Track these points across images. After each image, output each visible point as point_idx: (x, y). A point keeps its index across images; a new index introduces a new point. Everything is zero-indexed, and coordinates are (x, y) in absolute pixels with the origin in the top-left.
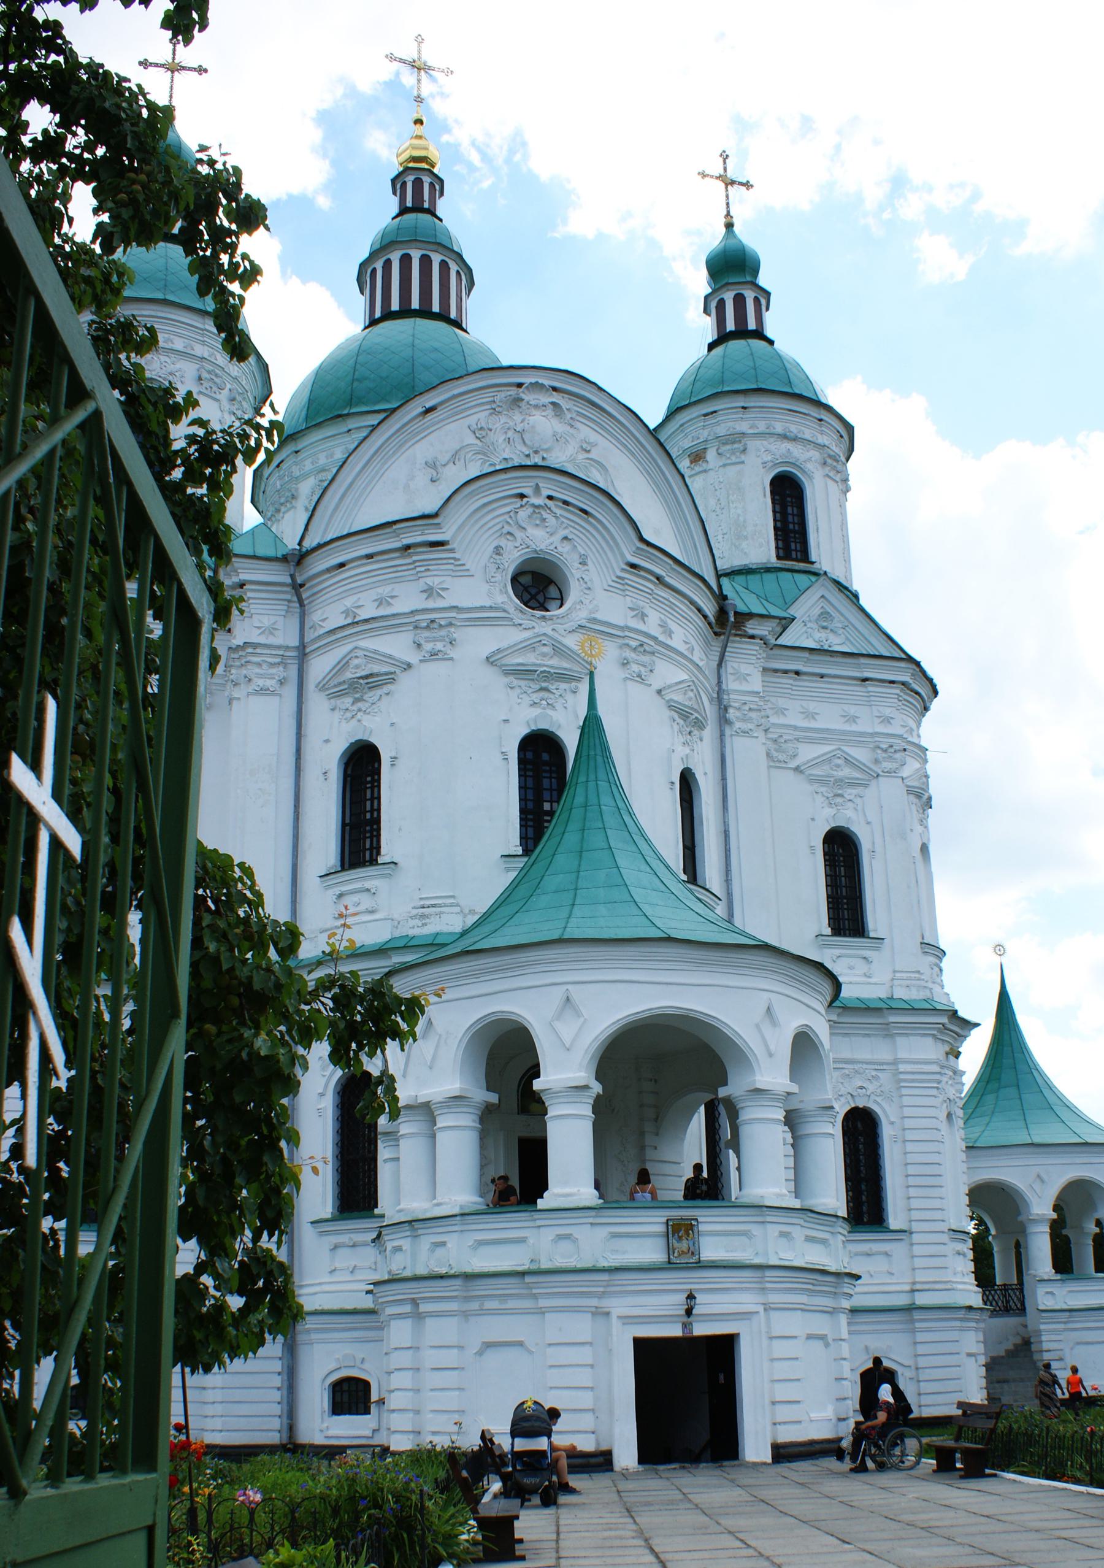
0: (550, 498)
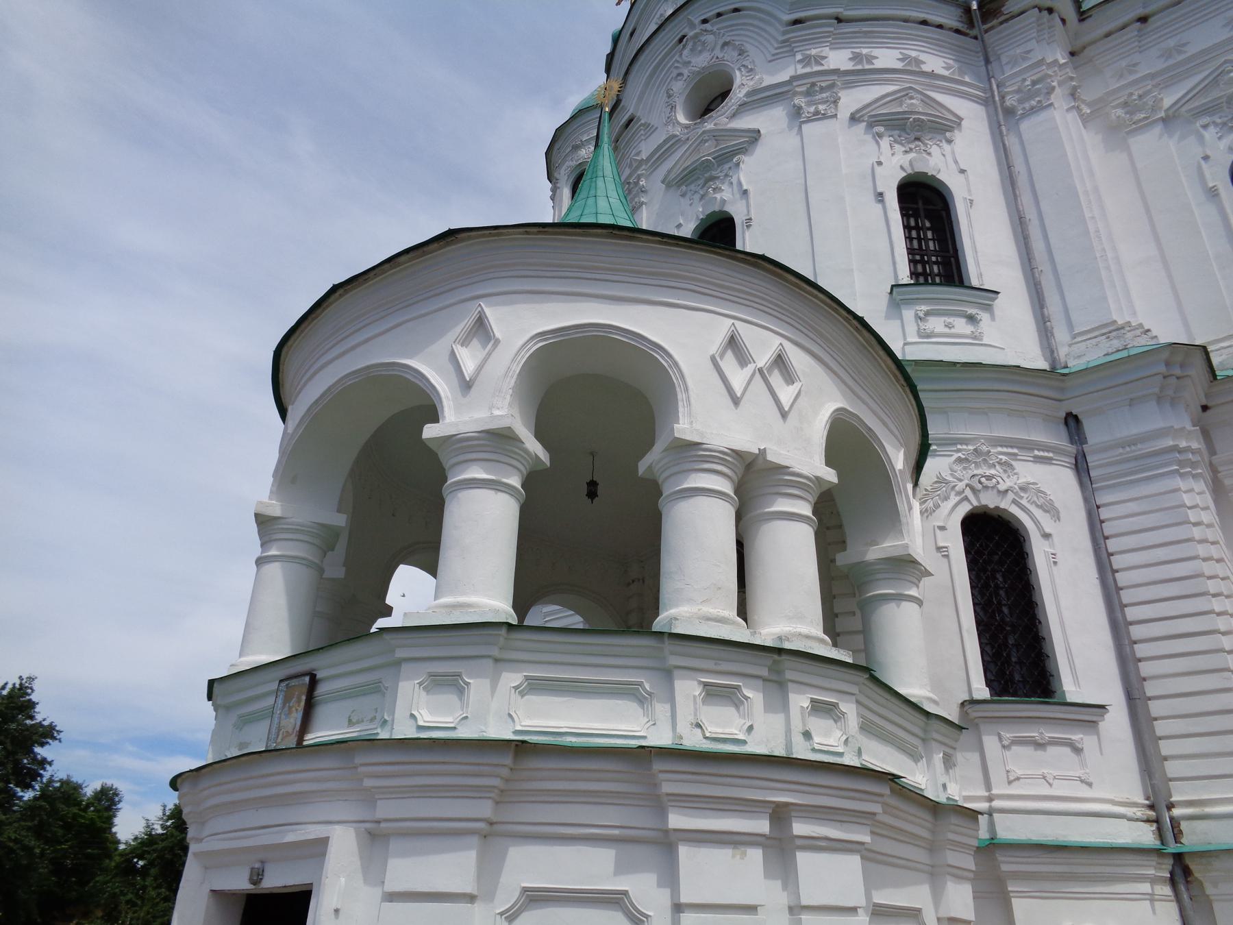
0: (705, 21)
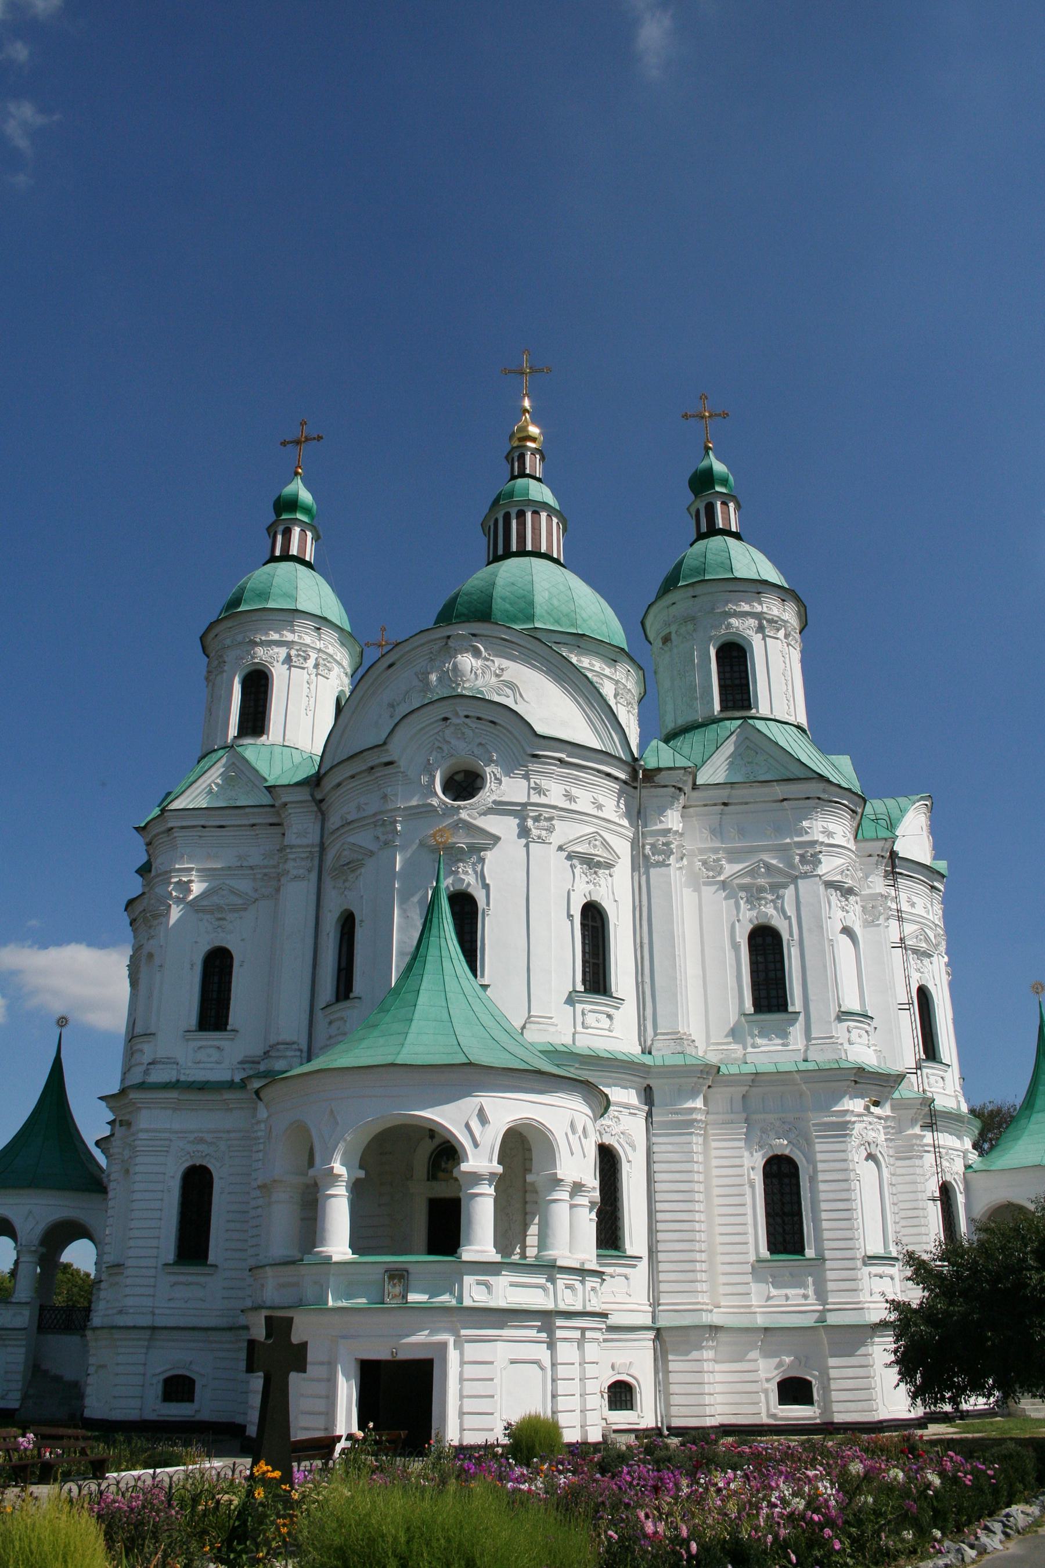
0: (467, 717)
